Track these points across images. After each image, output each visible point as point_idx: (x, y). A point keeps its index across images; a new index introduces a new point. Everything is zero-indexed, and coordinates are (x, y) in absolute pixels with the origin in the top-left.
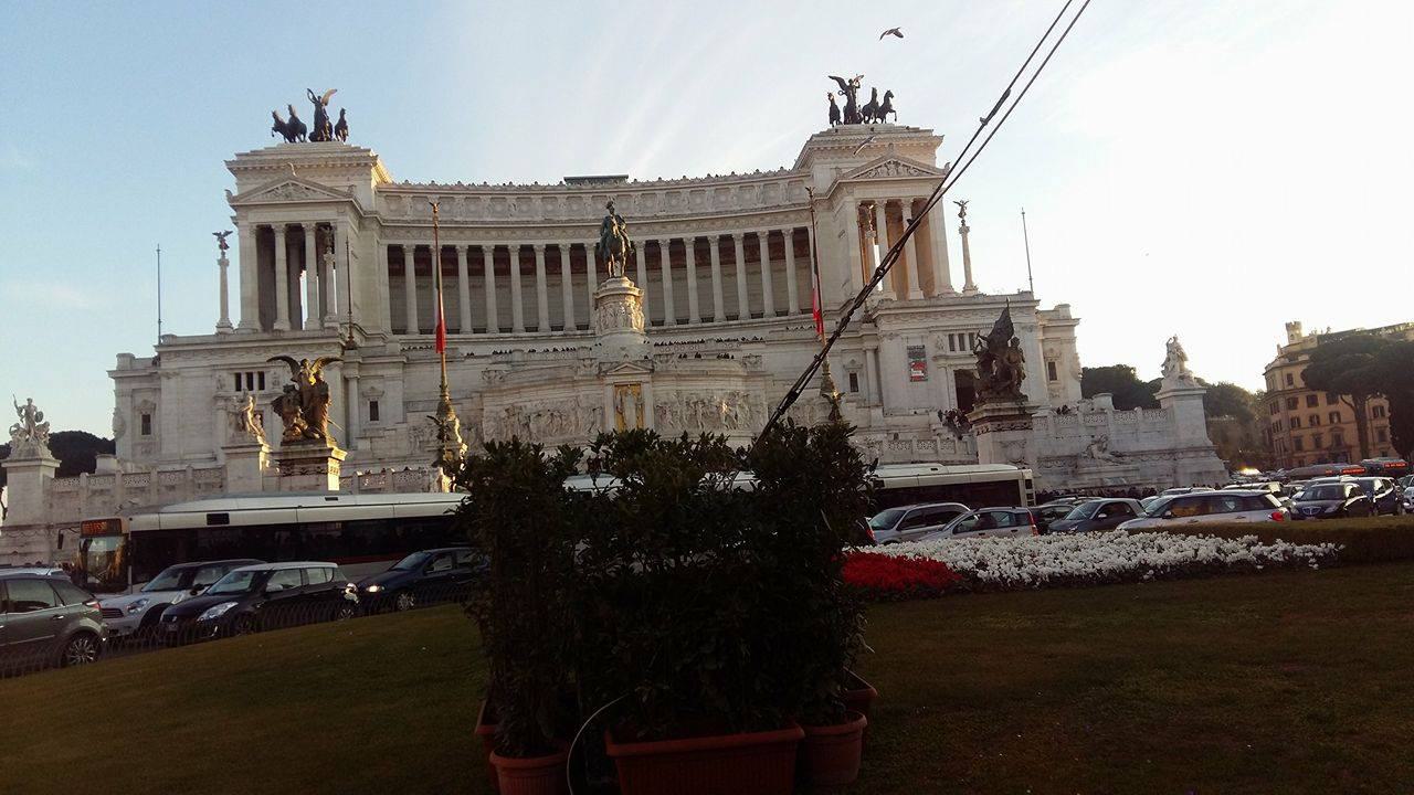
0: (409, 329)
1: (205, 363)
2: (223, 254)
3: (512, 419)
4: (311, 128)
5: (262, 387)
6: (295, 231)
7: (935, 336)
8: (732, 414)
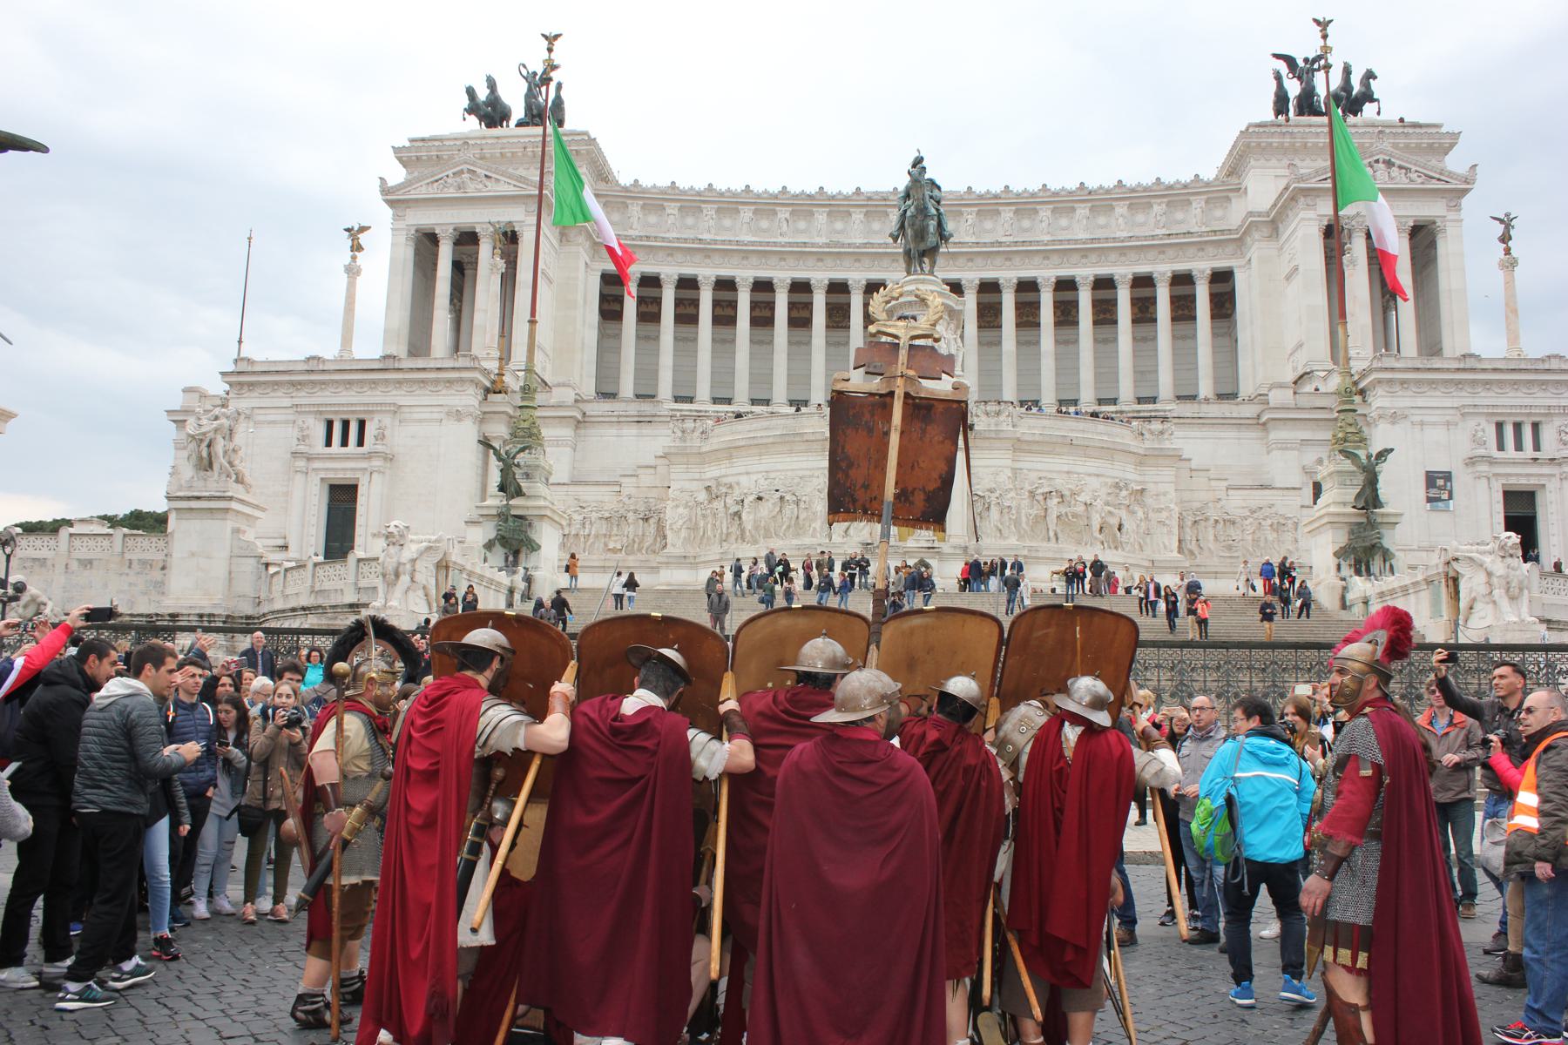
0: (621, 395)
1: (287, 402)
2: (354, 258)
3: (715, 504)
4: (518, 112)
5: (361, 443)
6: (467, 239)
7: (1471, 423)
8: (1114, 522)
